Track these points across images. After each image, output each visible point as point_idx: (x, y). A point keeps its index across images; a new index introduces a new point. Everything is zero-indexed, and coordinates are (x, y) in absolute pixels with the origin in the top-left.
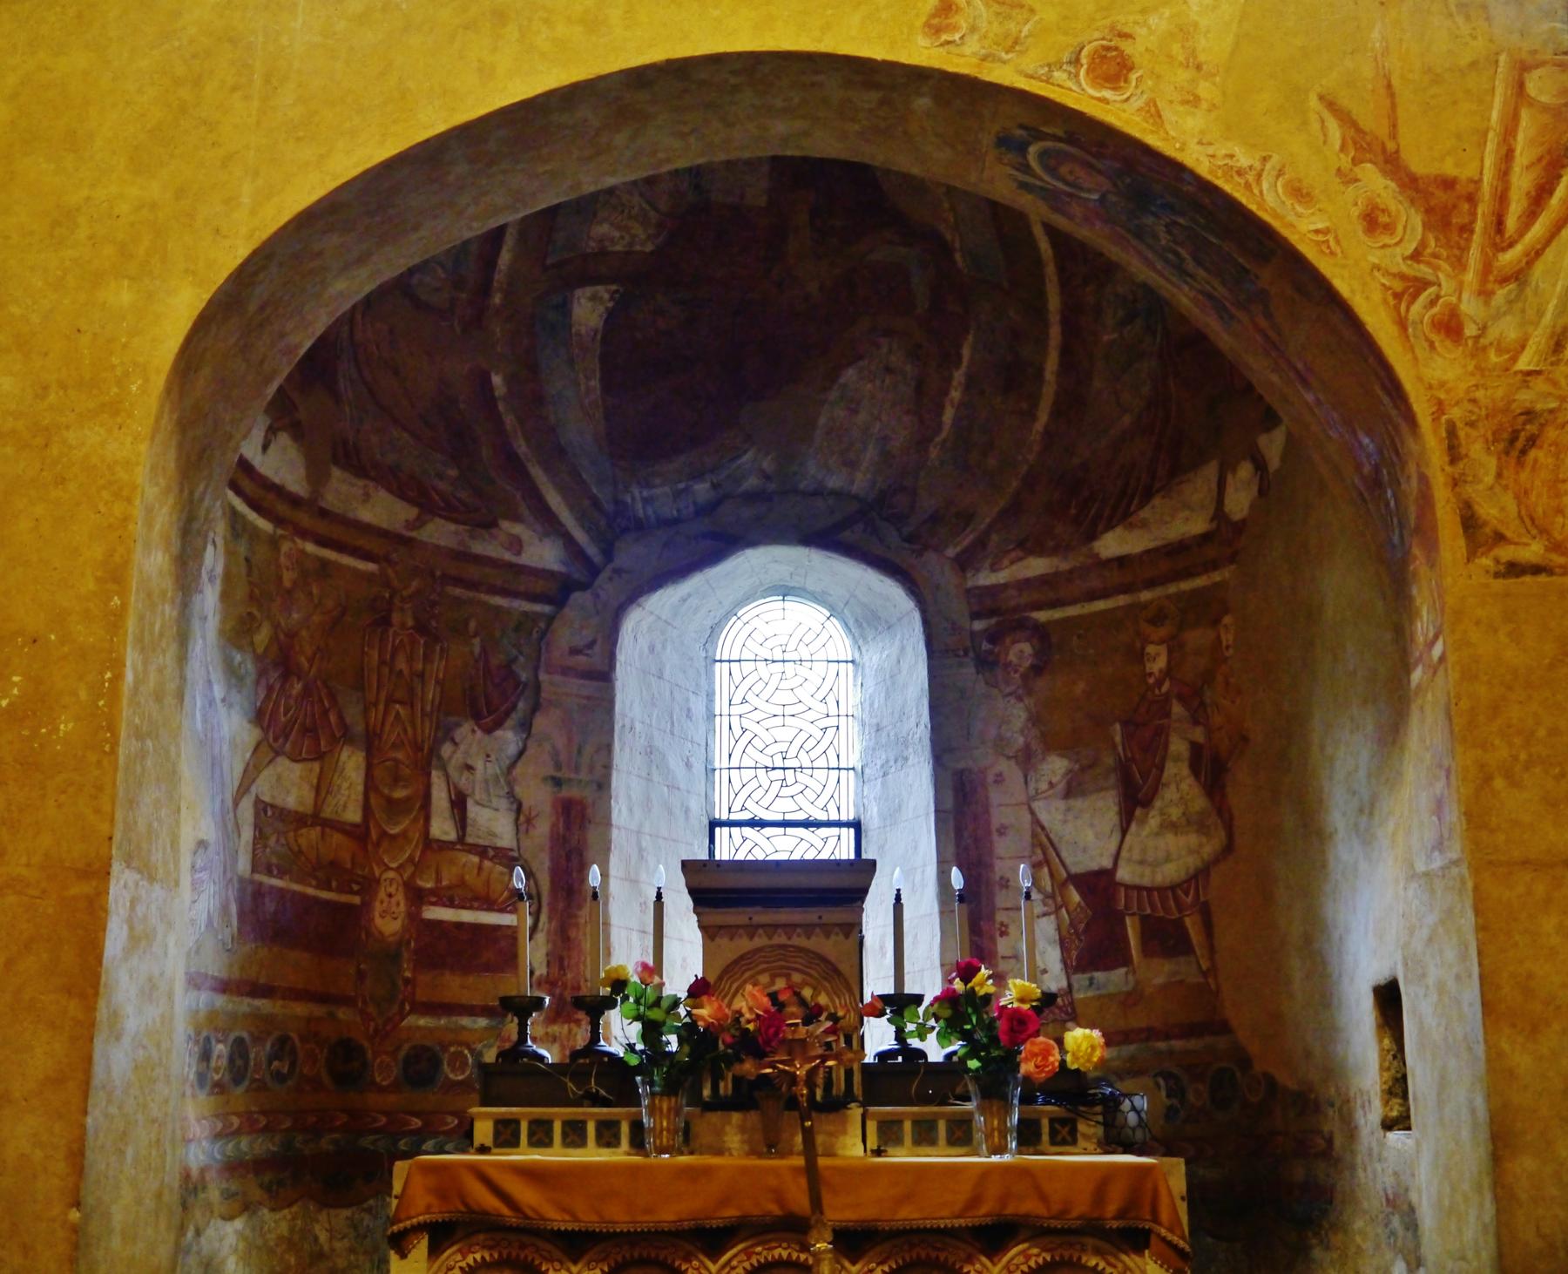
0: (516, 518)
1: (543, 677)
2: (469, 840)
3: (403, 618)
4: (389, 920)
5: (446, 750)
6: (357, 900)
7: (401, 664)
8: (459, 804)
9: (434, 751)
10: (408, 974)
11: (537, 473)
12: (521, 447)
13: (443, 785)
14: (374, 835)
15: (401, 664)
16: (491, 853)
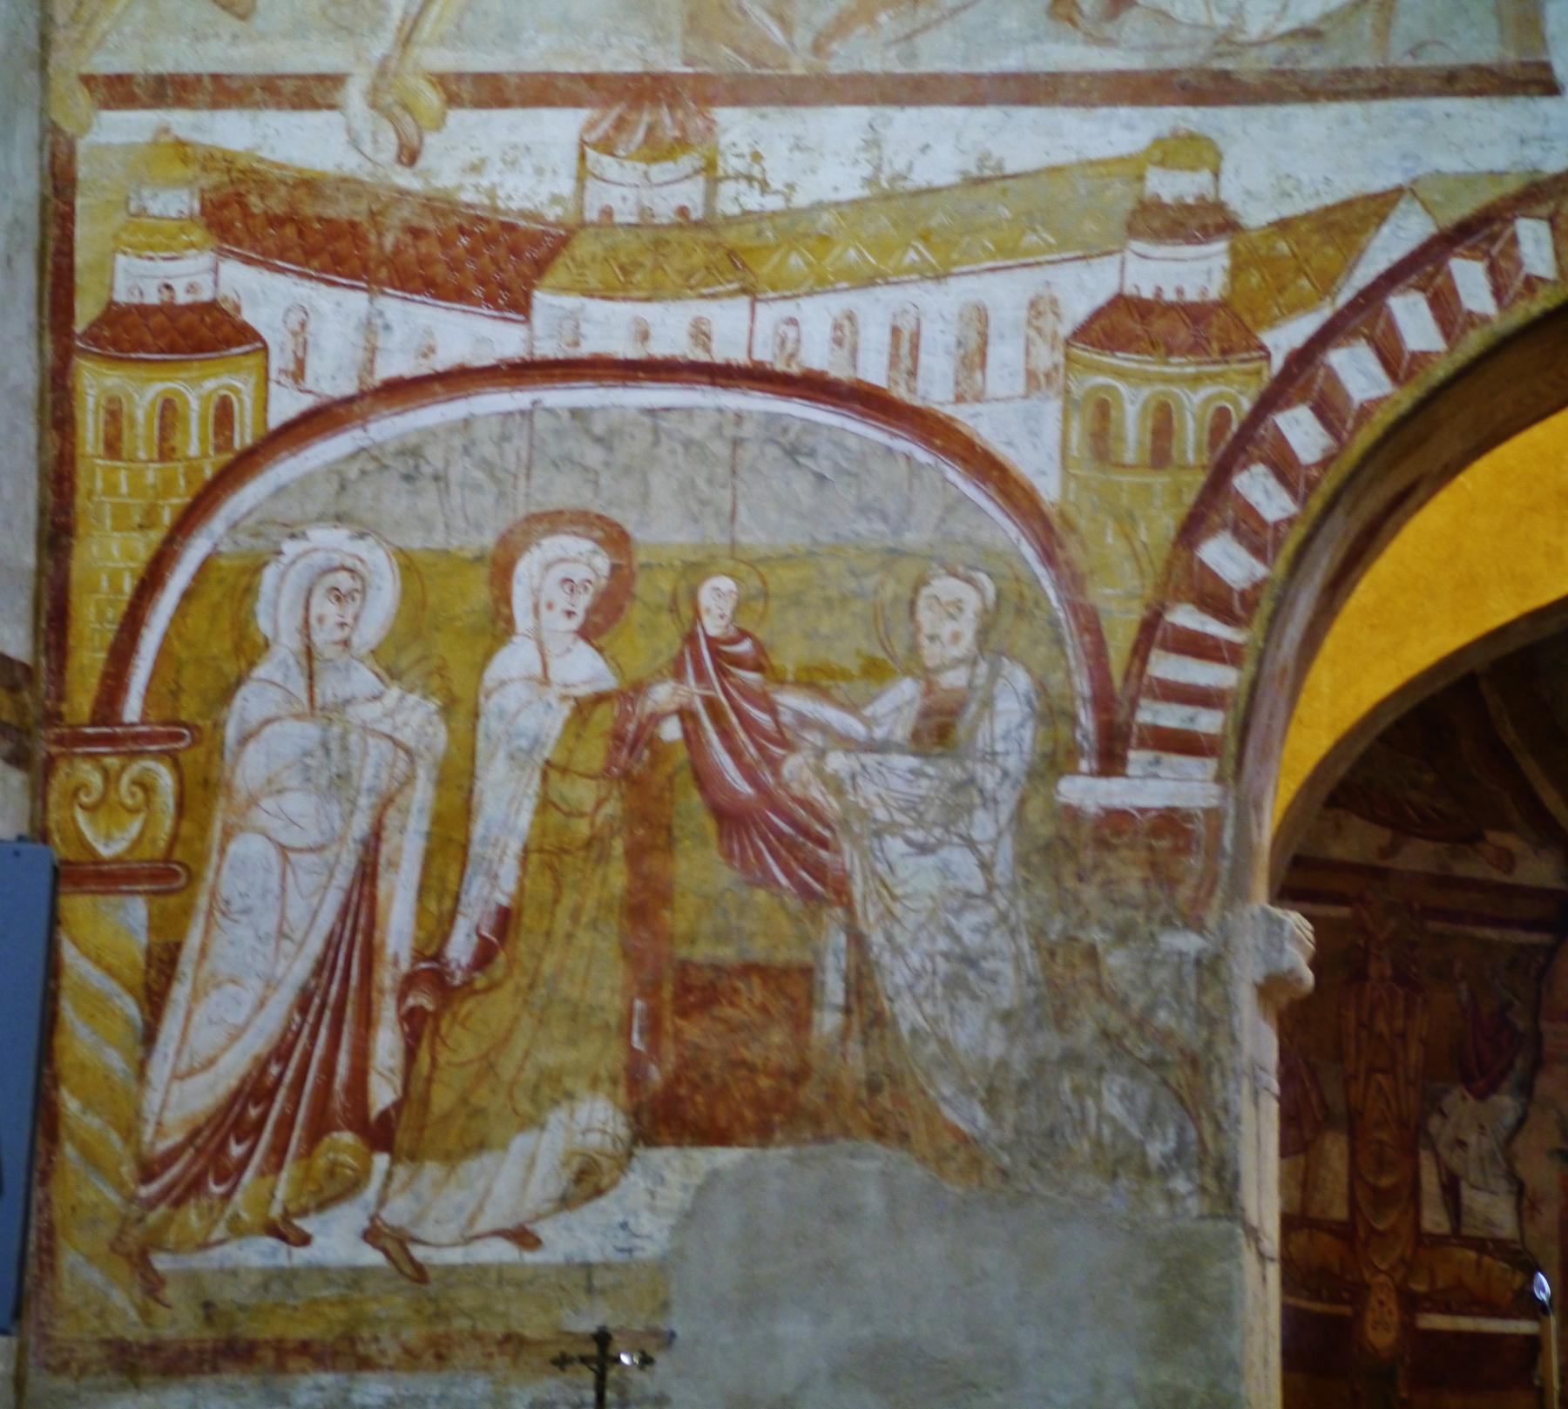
0: (1505, 826)
1: (1545, 1026)
2: (1466, 1231)
3: (1379, 968)
4: (1381, 1334)
5: (1434, 1123)
6: (1347, 1310)
7: (1381, 1026)
8: (1451, 1188)
9: (1422, 1128)
10: (1404, 1394)
11: (1530, 767)
12: (1509, 734)
13: (1434, 1170)
14: (1362, 1233)
15: (1381, 1026)
16: (1490, 1245)
